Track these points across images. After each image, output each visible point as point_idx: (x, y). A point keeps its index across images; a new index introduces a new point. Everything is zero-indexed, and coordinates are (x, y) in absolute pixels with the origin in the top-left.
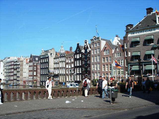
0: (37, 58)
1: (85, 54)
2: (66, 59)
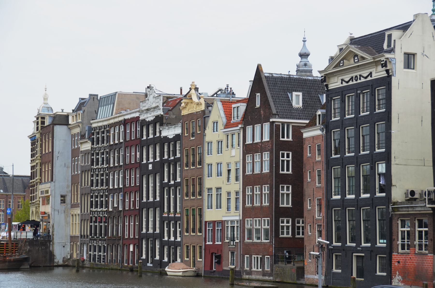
0: (300, 94)
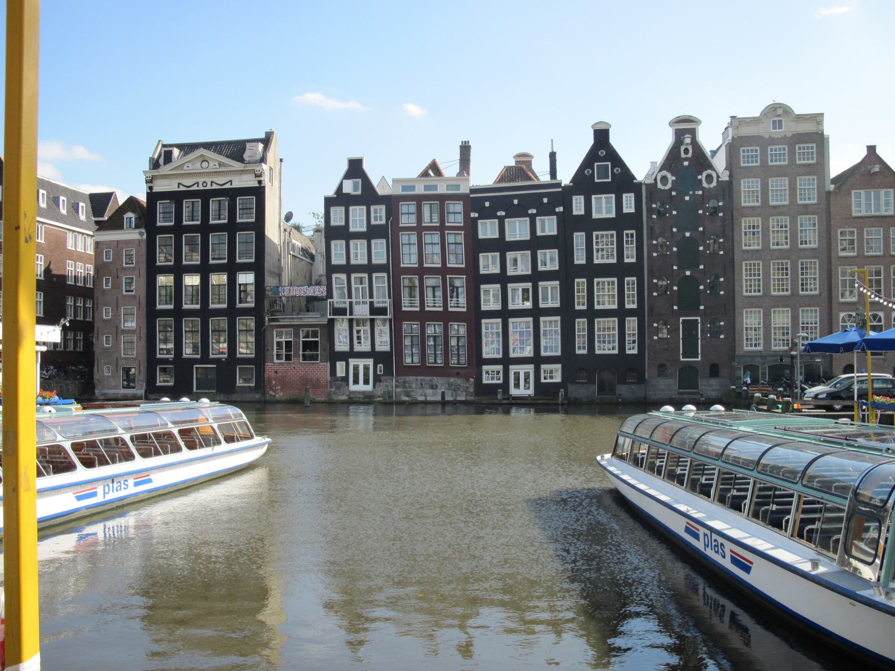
1: (681, 195)
2: (474, 215)
